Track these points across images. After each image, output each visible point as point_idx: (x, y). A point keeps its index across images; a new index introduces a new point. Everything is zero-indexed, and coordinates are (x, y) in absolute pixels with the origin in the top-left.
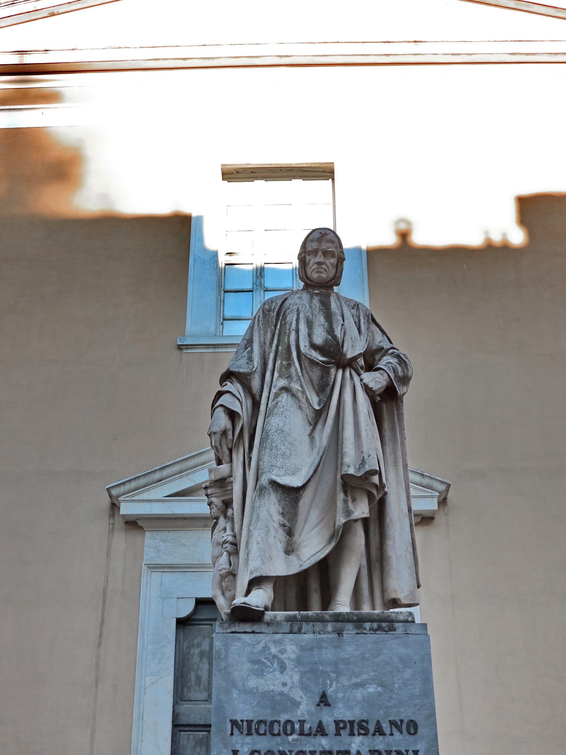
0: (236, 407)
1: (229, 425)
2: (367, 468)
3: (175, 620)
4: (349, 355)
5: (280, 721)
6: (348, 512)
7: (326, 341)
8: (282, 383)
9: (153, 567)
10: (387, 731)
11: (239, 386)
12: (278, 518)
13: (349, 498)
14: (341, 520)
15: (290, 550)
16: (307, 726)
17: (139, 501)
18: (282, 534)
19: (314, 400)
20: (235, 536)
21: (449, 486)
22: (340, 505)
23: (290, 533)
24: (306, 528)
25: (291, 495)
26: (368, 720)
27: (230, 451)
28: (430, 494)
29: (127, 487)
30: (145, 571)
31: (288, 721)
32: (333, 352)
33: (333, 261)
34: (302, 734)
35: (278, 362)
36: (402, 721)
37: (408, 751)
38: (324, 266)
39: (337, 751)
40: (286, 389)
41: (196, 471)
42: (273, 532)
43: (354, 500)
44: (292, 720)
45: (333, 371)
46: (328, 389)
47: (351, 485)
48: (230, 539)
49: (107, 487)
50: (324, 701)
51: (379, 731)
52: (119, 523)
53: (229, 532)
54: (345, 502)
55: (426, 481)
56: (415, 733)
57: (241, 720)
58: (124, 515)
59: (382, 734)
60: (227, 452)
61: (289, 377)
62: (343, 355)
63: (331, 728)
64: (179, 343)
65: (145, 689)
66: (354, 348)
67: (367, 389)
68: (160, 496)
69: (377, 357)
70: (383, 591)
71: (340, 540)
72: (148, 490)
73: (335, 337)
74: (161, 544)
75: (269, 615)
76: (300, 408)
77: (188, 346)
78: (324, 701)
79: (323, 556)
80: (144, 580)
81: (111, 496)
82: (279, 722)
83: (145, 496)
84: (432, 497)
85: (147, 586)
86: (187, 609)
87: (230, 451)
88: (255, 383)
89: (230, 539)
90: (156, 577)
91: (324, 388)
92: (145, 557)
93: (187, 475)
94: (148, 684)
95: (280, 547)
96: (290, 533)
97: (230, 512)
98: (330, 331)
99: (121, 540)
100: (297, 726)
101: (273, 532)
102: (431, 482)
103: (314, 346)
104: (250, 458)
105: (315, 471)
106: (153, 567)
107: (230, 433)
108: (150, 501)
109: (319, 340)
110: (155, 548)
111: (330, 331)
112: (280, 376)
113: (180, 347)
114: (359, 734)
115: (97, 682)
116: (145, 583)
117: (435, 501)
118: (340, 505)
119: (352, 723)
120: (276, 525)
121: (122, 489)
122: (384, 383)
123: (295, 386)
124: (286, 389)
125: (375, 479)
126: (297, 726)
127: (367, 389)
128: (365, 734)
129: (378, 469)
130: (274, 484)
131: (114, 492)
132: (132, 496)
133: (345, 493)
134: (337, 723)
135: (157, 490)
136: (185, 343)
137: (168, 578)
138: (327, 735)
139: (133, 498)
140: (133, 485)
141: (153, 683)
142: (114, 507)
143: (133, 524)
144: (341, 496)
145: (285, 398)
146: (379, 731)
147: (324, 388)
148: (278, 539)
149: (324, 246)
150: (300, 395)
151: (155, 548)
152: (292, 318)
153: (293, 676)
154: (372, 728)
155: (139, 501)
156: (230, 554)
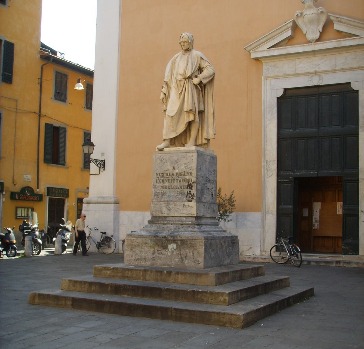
3: (276, 98)
10: (186, 174)
16: (170, 174)
17: (259, 51)
30: (264, 80)
31: (167, 173)
34: (169, 176)
38: (185, 46)
50: (174, 168)
51: (184, 175)
56: (192, 175)
58: (253, 58)
63: (175, 174)
65: (267, 125)
75: (166, 149)
78: (174, 168)
80: (263, 83)
83: (260, 49)
85: (265, 85)
86: (280, 93)
90: (268, 81)
92: (264, 74)
94: (267, 124)
100: (168, 174)
110: (267, 69)
114: (180, 175)
116: (264, 85)
126: (168, 174)
128: (182, 175)
132: (254, 50)
134: (176, 173)
137: (273, 81)
139: (255, 51)
141: (269, 124)
146: (184, 175)
149: (183, 40)
151: (267, 69)
153: (169, 163)
154: (183, 174)
155: (259, 51)
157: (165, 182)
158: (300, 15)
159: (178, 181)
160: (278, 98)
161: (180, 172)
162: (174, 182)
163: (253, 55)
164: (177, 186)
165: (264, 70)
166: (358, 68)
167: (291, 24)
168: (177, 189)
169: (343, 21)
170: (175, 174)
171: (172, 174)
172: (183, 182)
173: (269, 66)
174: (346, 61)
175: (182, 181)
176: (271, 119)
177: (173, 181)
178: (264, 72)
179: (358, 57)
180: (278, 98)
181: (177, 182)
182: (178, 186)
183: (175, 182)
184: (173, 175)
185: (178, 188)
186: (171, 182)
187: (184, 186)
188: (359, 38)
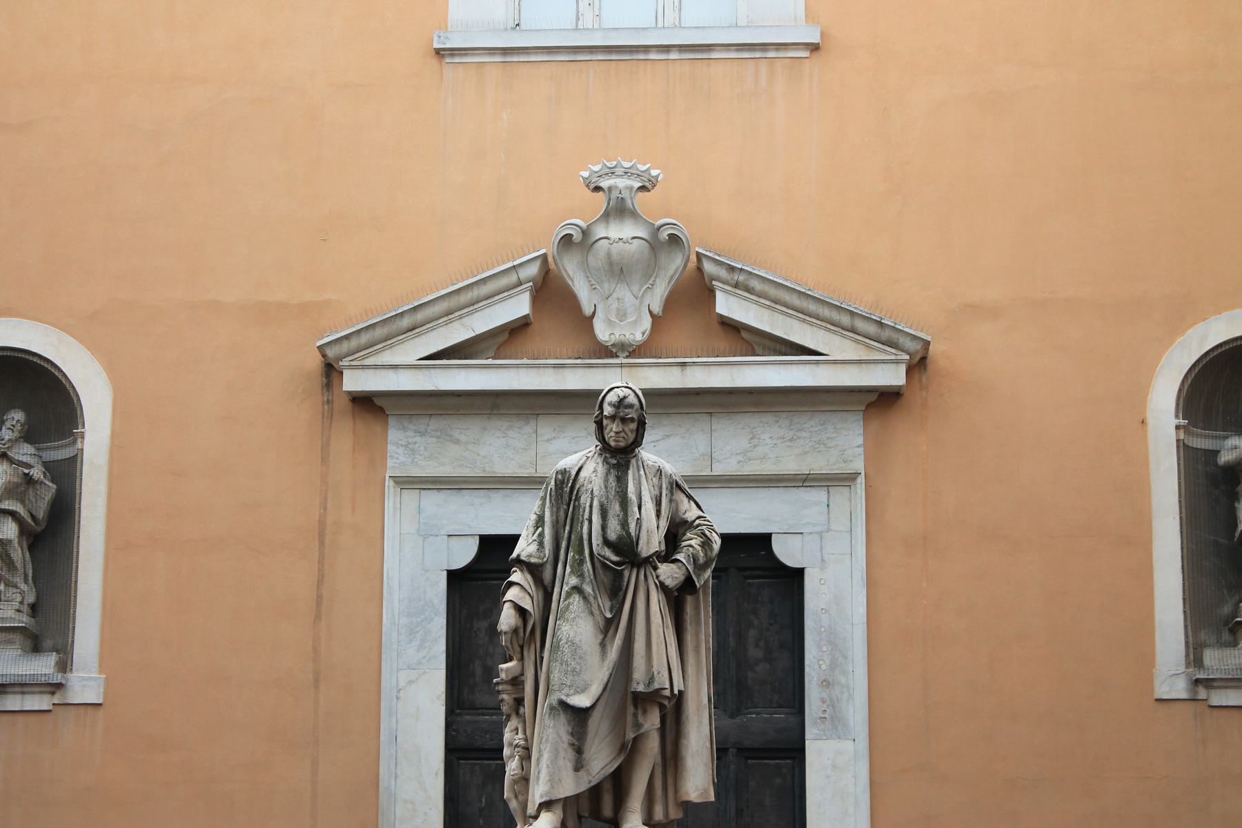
0: (527, 604)
1: (520, 623)
2: (656, 686)
4: (644, 554)
6: (638, 725)
7: (620, 538)
8: (573, 581)
9: (406, 483)
11: (529, 577)
12: (566, 738)
13: (640, 712)
14: (631, 735)
15: (578, 766)
17: (376, 367)
18: (571, 754)
19: (605, 603)
20: (526, 740)
21: (927, 344)
22: (630, 718)
23: (579, 751)
24: (596, 741)
25: (579, 716)
27: (522, 647)
28: (893, 357)
29: (354, 343)
32: (626, 548)
33: (633, 426)
35: (571, 554)
40: (577, 589)
41: (476, 311)
42: (562, 754)
43: (645, 712)
45: (626, 573)
46: (621, 593)
47: (642, 700)
48: (522, 742)
49: (319, 344)
52: (342, 403)
53: (520, 735)
54: (635, 715)
55: (886, 334)
58: (349, 393)
60: (518, 649)
61: (581, 576)
62: (636, 554)
64: (437, 46)
66: (652, 541)
67: (663, 587)
68: (411, 359)
69: (681, 531)
70: (676, 791)
71: (629, 751)
72: (391, 346)
73: (629, 534)
74: (418, 439)
76: (592, 613)
77: (454, 52)
79: (616, 766)
80: (389, 504)
81: (324, 356)
83: (387, 357)
84: (897, 362)
86: (465, 553)
87: (522, 647)
88: (547, 574)
89: (522, 742)
90: (410, 497)
91: (616, 591)
92: (390, 463)
93: (461, 317)
94: (402, 684)
95: (570, 766)
96: (579, 751)
97: (521, 711)
98: (624, 524)
99: (345, 434)
101: (562, 754)
102: (894, 336)
103: (607, 542)
104: (542, 658)
105: (604, 689)
106: (406, 483)
107: (521, 631)
108: (395, 367)
109: (612, 536)
110: (406, 446)
111: (624, 524)
112: (572, 572)
113: (438, 52)
115: (317, 681)
117: (903, 369)
118: (630, 718)
120: (566, 745)
121: (345, 346)
122: (682, 578)
123: (588, 589)
124: (577, 589)
125: (667, 693)
127: (663, 587)
129: (667, 686)
130: (563, 705)
131: (331, 353)
133: (636, 707)
135: (408, 346)
136: (448, 46)
137: (432, 501)
139: (368, 362)
140: (364, 338)
141: (410, 682)
142: (331, 371)
143: (366, 403)
144: (631, 709)
145: (576, 598)
147: (616, 591)
148: (566, 764)
150: (592, 599)
151: (406, 446)
152: (585, 499)
155: (376, 367)
156: (522, 759)
158: (577, 236)
160: (452, 576)
163: (354, 381)
165: (390, 448)
166: (805, 480)
167: (533, 270)
169: (755, 284)
173: (416, 431)
174: (755, 446)
176: (419, 663)
178: (392, 457)
179: (804, 434)
180: (452, 576)
188: (817, 362)
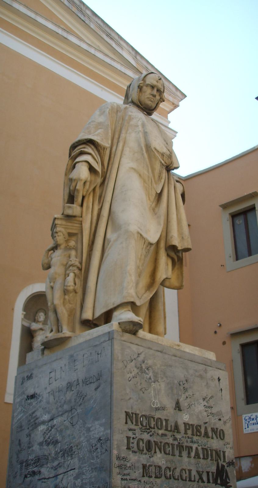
5: (155, 417)
10: (210, 434)
26: (201, 425)
36: (217, 429)
37: (221, 451)
39: (186, 446)
44: (162, 418)
50: (178, 407)
51: (206, 435)
57: (132, 413)
59: (208, 437)
63: (182, 428)
78: (178, 407)
82: (154, 418)
100: (164, 423)
119: (192, 425)
128: (200, 436)
138: (180, 433)
146: (206, 435)
153: (162, 386)
157: (155, 452)
159: (193, 454)
161: (195, 422)
162: (180, 456)
164: (190, 471)
168: (190, 480)
170: (182, 428)
171: (173, 424)
172: (204, 458)
175: (201, 456)
177: (177, 453)
181: (189, 456)
182: (194, 473)
183: (185, 454)
184: (177, 428)
185: (193, 479)
186: (173, 455)
187: (208, 473)
